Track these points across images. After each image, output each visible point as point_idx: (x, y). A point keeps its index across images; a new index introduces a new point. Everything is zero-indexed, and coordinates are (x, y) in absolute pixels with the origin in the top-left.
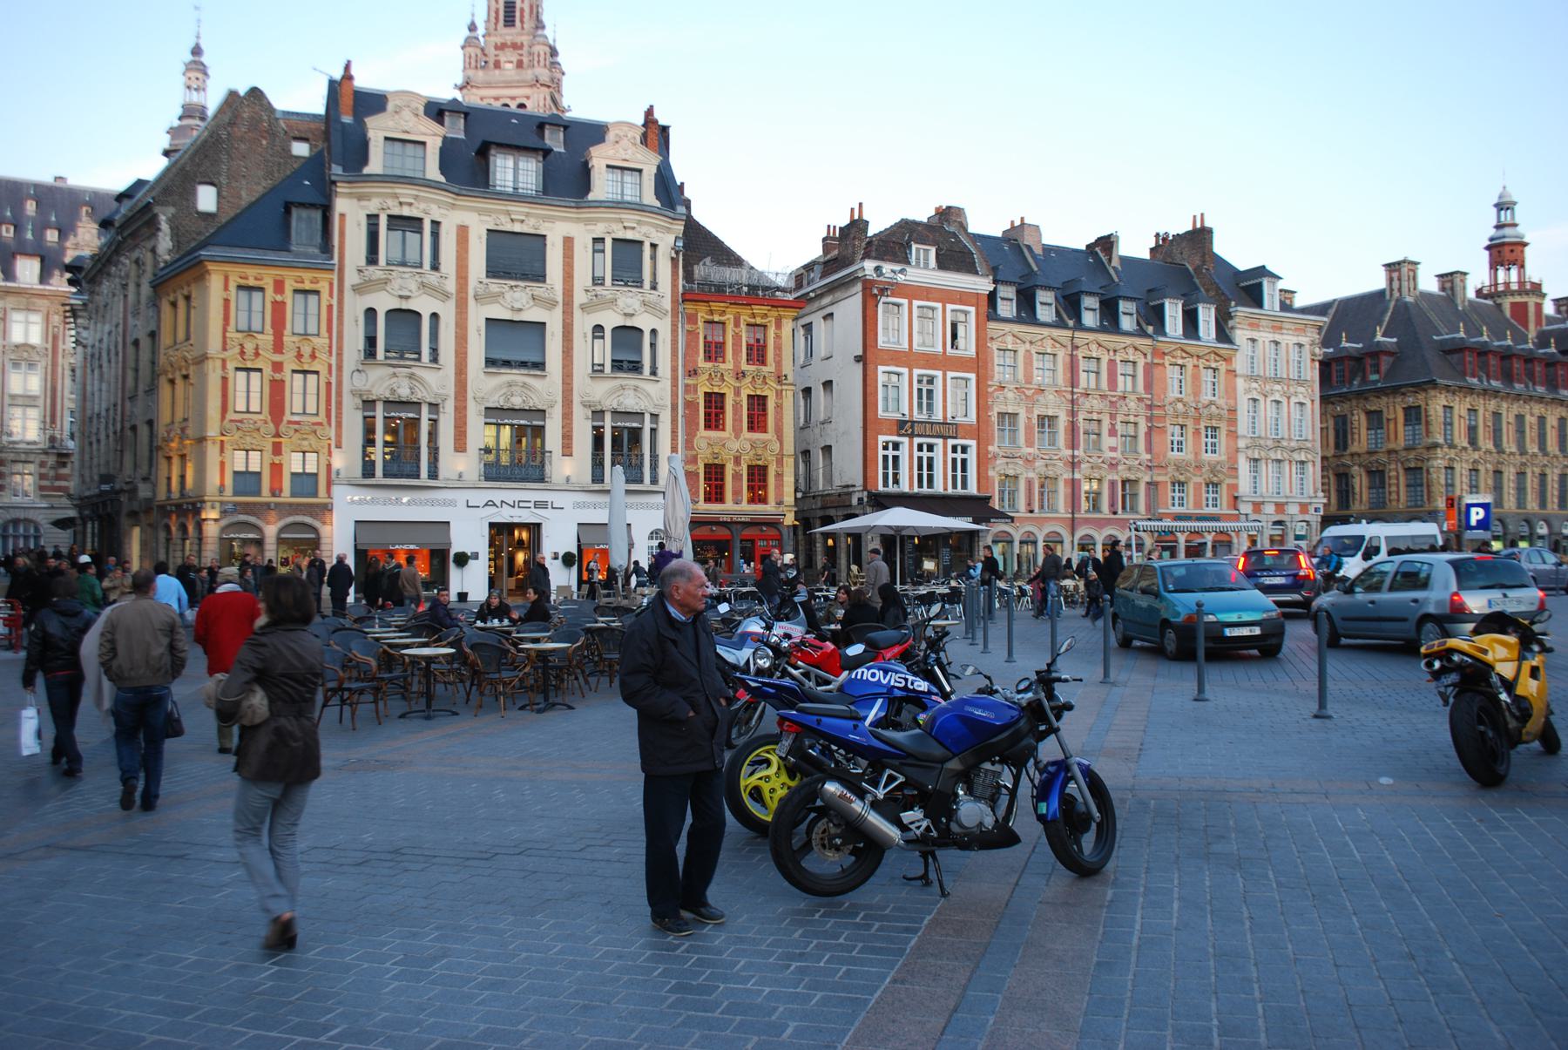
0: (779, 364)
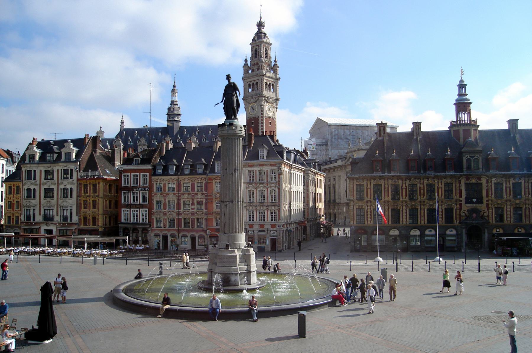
0: (99, 192)
